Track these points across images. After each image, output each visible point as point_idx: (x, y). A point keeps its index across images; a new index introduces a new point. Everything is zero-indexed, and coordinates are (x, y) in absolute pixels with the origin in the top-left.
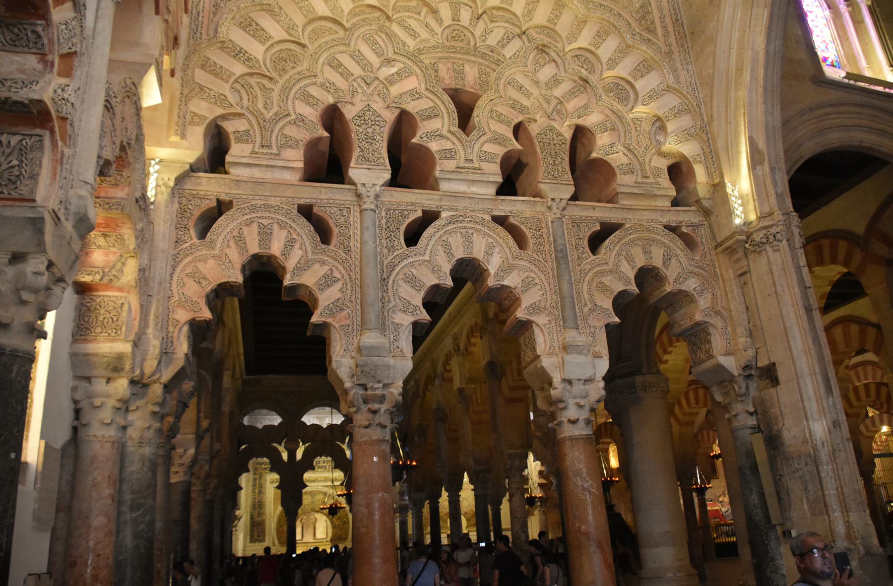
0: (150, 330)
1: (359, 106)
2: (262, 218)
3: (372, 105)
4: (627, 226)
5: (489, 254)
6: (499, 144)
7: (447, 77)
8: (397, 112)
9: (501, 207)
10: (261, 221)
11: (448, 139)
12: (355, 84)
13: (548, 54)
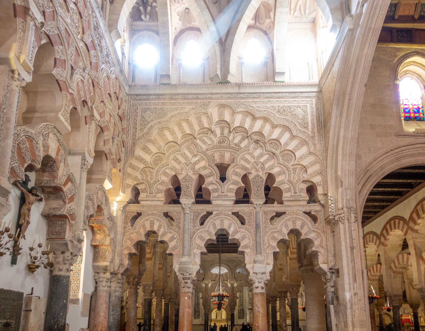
0: (116, 257)
1: (184, 174)
2: (151, 218)
3: (189, 174)
4: (287, 213)
5: (230, 227)
6: (236, 185)
7: (217, 159)
8: (197, 175)
9: (235, 209)
10: (151, 219)
11: (215, 184)
12: (183, 166)
13: (259, 144)
